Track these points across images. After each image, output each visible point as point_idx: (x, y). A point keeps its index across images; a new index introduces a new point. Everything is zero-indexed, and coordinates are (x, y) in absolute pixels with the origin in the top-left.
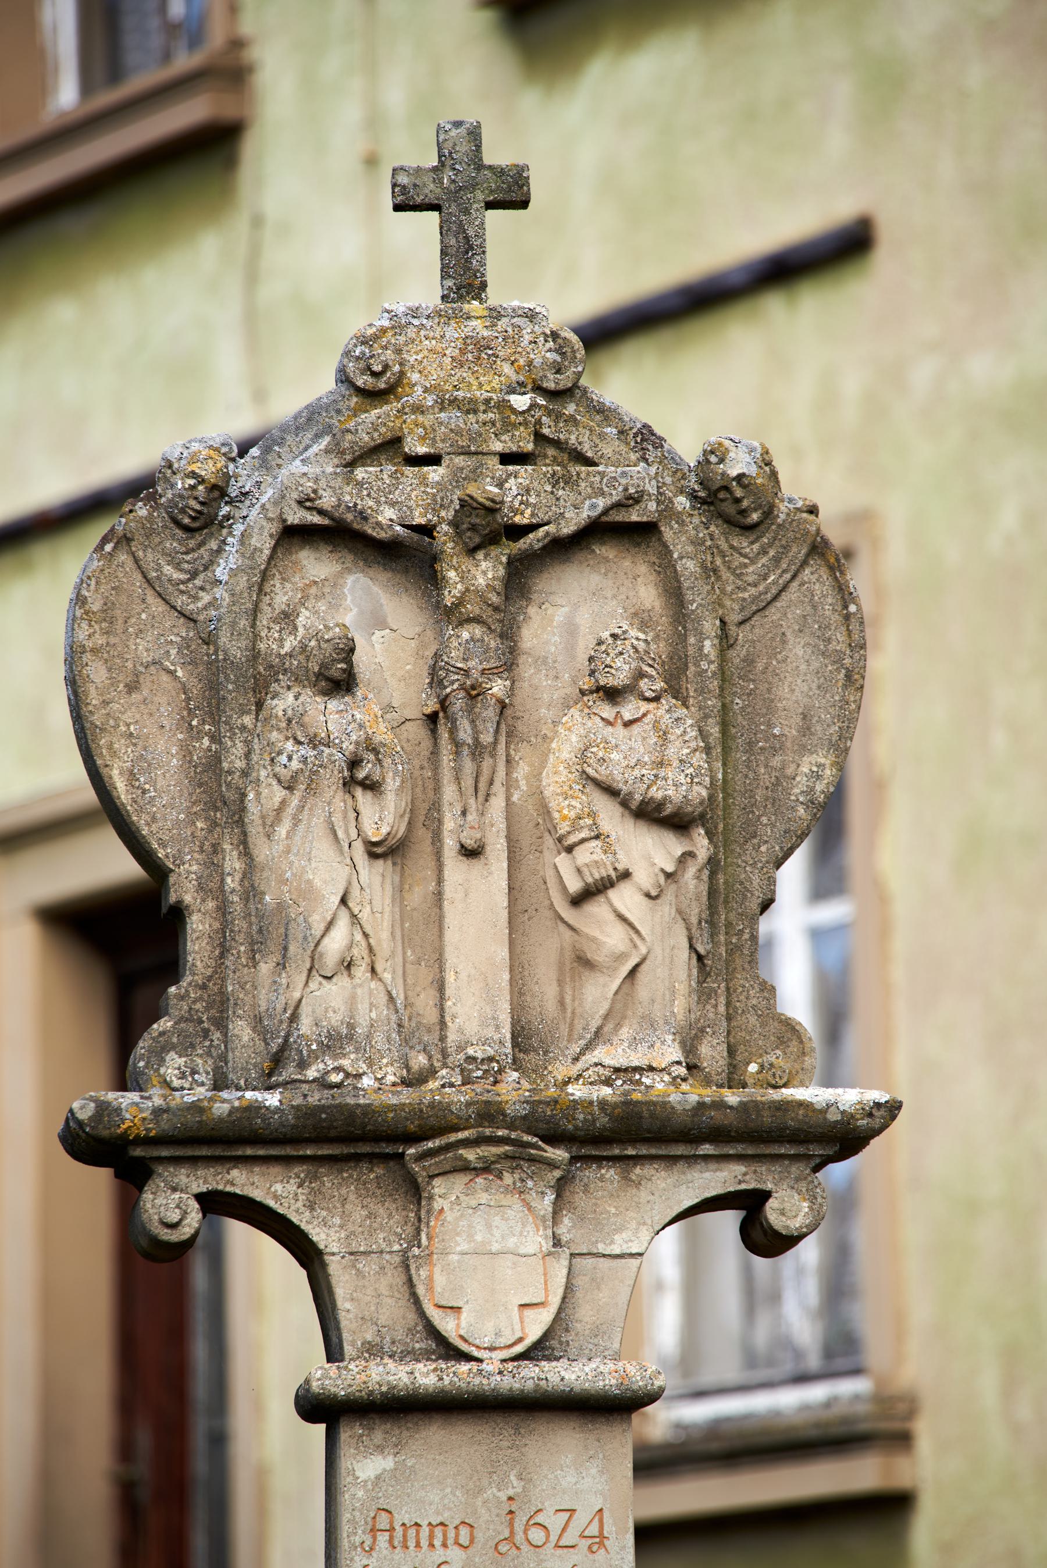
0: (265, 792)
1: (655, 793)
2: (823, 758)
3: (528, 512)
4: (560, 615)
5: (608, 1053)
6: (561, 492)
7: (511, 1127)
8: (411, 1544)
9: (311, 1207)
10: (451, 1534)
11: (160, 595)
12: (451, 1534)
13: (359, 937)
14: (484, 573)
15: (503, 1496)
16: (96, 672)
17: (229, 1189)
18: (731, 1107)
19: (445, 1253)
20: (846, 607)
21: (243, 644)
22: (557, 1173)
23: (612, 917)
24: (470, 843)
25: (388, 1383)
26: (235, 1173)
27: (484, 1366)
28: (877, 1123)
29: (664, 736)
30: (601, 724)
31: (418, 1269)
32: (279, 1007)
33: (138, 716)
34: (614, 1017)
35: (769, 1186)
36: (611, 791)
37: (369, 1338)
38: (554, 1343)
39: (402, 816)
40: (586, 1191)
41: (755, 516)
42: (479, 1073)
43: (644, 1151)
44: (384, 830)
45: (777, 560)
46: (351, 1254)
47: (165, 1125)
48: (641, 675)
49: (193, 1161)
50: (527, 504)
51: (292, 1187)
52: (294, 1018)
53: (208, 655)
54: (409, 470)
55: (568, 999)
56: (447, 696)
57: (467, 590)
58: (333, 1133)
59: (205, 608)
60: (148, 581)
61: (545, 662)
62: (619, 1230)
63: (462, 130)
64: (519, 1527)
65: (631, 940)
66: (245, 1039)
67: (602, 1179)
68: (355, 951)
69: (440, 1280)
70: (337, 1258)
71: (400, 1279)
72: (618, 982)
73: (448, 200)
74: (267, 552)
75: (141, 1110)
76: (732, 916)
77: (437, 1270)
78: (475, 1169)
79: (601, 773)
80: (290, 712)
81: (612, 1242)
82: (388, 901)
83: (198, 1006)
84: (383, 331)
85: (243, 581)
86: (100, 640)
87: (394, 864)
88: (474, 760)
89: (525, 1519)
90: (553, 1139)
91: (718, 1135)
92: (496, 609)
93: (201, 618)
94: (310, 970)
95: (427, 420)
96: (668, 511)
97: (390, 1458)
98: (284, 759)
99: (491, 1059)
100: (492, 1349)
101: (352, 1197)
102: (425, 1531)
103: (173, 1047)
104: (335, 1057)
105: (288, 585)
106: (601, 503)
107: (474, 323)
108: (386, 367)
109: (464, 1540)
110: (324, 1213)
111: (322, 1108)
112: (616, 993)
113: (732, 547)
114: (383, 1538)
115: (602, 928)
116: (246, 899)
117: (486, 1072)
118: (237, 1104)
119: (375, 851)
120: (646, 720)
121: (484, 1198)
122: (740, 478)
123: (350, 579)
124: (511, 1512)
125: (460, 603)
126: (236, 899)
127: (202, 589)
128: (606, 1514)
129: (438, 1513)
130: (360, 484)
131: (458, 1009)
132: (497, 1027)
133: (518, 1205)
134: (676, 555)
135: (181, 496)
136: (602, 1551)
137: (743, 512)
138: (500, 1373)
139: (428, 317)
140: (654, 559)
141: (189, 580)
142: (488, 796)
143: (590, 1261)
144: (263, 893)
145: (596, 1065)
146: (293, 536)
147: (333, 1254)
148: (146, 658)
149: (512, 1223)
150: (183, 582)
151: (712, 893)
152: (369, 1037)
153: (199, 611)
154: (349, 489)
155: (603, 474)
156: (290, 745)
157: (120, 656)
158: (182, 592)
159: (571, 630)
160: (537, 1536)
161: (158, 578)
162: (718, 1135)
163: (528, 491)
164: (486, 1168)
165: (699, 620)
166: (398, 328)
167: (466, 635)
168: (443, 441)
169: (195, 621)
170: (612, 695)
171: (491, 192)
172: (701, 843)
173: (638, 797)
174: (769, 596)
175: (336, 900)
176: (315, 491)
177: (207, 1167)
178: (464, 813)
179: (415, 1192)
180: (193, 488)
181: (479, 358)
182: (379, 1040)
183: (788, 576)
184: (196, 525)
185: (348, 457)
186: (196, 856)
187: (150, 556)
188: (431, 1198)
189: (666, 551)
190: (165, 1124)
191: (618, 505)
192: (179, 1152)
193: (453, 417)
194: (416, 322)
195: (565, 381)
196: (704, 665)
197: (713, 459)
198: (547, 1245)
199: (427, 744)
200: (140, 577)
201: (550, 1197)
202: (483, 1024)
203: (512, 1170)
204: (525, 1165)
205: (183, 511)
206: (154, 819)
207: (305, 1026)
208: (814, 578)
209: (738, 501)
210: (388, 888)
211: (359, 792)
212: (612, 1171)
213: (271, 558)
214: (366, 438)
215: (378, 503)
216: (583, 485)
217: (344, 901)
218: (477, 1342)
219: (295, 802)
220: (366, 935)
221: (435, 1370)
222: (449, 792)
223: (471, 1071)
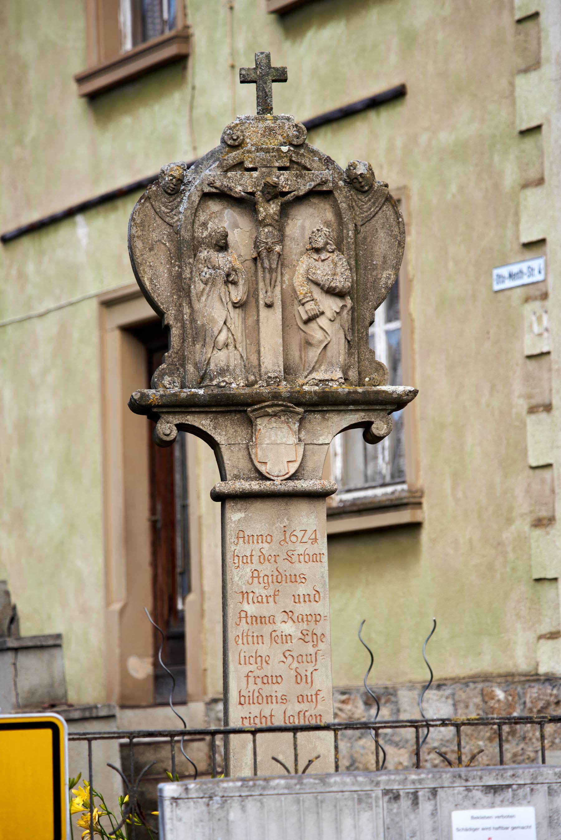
0: (197, 285)
1: (333, 285)
2: (391, 272)
3: (288, 187)
4: (299, 223)
5: (317, 375)
6: (299, 180)
7: (284, 401)
8: (251, 542)
10: (264, 538)
11: (160, 217)
12: (264, 538)
13: (230, 335)
14: (273, 208)
15: (282, 526)
16: (139, 244)
17: (187, 422)
18: (360, 393)
19: (261, 444)
20: (398, 219)
21: (189, 234)
22: (300, 416)
23: (318, 328)
24: (268, 302)
25: (242, 488)
26: (189, 417)
27: (275, 482)
28: (410, 397)
29: (336, 264)
30: (314, 261)
31: (252, 449)
32: (203, 360)
33: (153, 260)
34: (319, 362)
35: (373, 420)
36: (317, 284)
37: (235, 473)
38: (299, 474)
39: (245, 293)
40: (310, 422)
41: (366, 188)
42: (272, 382)
43: (330, 408)
44: (239, 298)
45: (374, 203)
47: (164, 401)
48: (327, 243)
49: (174, 413)
50: (287, 184)
51: (208, 422)
52: (208, 363)
53: (177, 238)
54: (246, 173)
55: (303, 356)
56: (260, 251)
57: (267, 214)
58: (222, 403)
59: (176, 222)
60: (156, 212)
61: (294, 239)
62: (321, 435)
63: (264, 55)
65: (325, 336)
66: (192, 371)
67: (315, 418)
68: (229, 340)
69: (260, 453)
71: (246, 453)
72: (320, 350)
73: (259, 79)
74: (197, 202)
75: (156, 396)
76: (360, 327)
77: (258, 450)
79: (314, 278)
80: (206, 258)
81: (319, 440)
82: (240, 323)
83: (175, 360)
84: (237, 125)
85: (189, 212)
86: (140, 233)
87: (242, 310)
88: (269, 274)
89: (289, 533)
90: (298, 404)
91: (355, 402)
92: (277, 221)
93: (175, 225)
94: (214, 347)
95: (252, 155)
96: (336, 186)
97: (243, 513)
98: (204, 274)
99: (276, 377)
100: (278, 476)
101: (229, 425)
102: (255, 538)
103: (167, 374)
104: (223, 377)
105: (205, 213)
106: (313, 184)
107: (268, 122)
108: (238, 137)
109: (269, 540)
110: (219, 431)
111: (218, 395)
112: (320, 354)
113: (359, 199)
114: (241, 540)
115: (315, 332)
116: (191, 322)
117: (275, 382)
118: (189, 393)
119: (236, 306)
120: (329, 259)
121: (274, 425)
122: (361, 174)
123: (226, 211)
124: (285, 531)
125: (264, 219)
126: (188, 323)
127: (175, 215)
128: (317, 531)
129: (260, 532)
130: (229, 178)
131: (265, 360)
132: (279, 366)
133: (286, 427)
134: (339, 202)
135: (167, 183)
136: (316, 544)
137: (362, 187)
138: (281, 484)
139: (252, 120)
140: (331, 203)
141: (170, 212)
142: (274, 287)
143: (311, 446)
144: (197, 321)
145: (313, 379)
146: (206, 196)
148: (156, 239)
149: (284, 433)
150: (168, 213)
151: (353, 319)
152: (234, 370)
153: (174, 223)
154: (225, 180)
155: (313, 174)
156: (206, 269)
157: (147, 239)
158: (168, 216)
159: (303, 228)
160: (294, 539)
161: (160, 211)
162: (355, 402)
163: (288, 180)
164: (275, 415)
165: (347, 224)
166: (242, 124)
167: (266, 230)
168: (258, 163)
169: (173, 226)
170: (317, 251)
171: (274, 76)
172: (349, 302)
173: (327, 286)
174: (371, 216)
175: (222, 323)
176: (214, 181)
177: (179, 415)
178: (266, 292)
179: (251, 423)
180: (171, 180)
181: (270, 134)
182: (238, 371)
183: (378, 209)
184: (173, 193)
185: (225, 169)
186: (174, 308)
187: (157, 204)
188: (256, 425)
189: (336, 200)
190: (164, 400)
191: (319, 185)
192: (169, 410)
193: (262, 154)
194: (248, 121)
195: (300, 141)
196: (349, 240)
197: (352, 168)
198: (296, 441)
199: (253, 268)
200: (153, 211)
202: (274, 365)
203: (284, 415)
205: (168, 188)
206: (159, 295)
207: (212, 366)
208: (387, 209)
209: (360, 183)
210: (240, 318)
211: (230, 285)
212: (319, 415)
213: (199, 204)
214: (231, 162)
215: (236, 184)
216: (307, 177)
217: (225, 323)
218: (273, 474)
219: (208, 289)
220: (233, 335)
221: (258, 484)
222: (261, 285)
223: (270, 381)
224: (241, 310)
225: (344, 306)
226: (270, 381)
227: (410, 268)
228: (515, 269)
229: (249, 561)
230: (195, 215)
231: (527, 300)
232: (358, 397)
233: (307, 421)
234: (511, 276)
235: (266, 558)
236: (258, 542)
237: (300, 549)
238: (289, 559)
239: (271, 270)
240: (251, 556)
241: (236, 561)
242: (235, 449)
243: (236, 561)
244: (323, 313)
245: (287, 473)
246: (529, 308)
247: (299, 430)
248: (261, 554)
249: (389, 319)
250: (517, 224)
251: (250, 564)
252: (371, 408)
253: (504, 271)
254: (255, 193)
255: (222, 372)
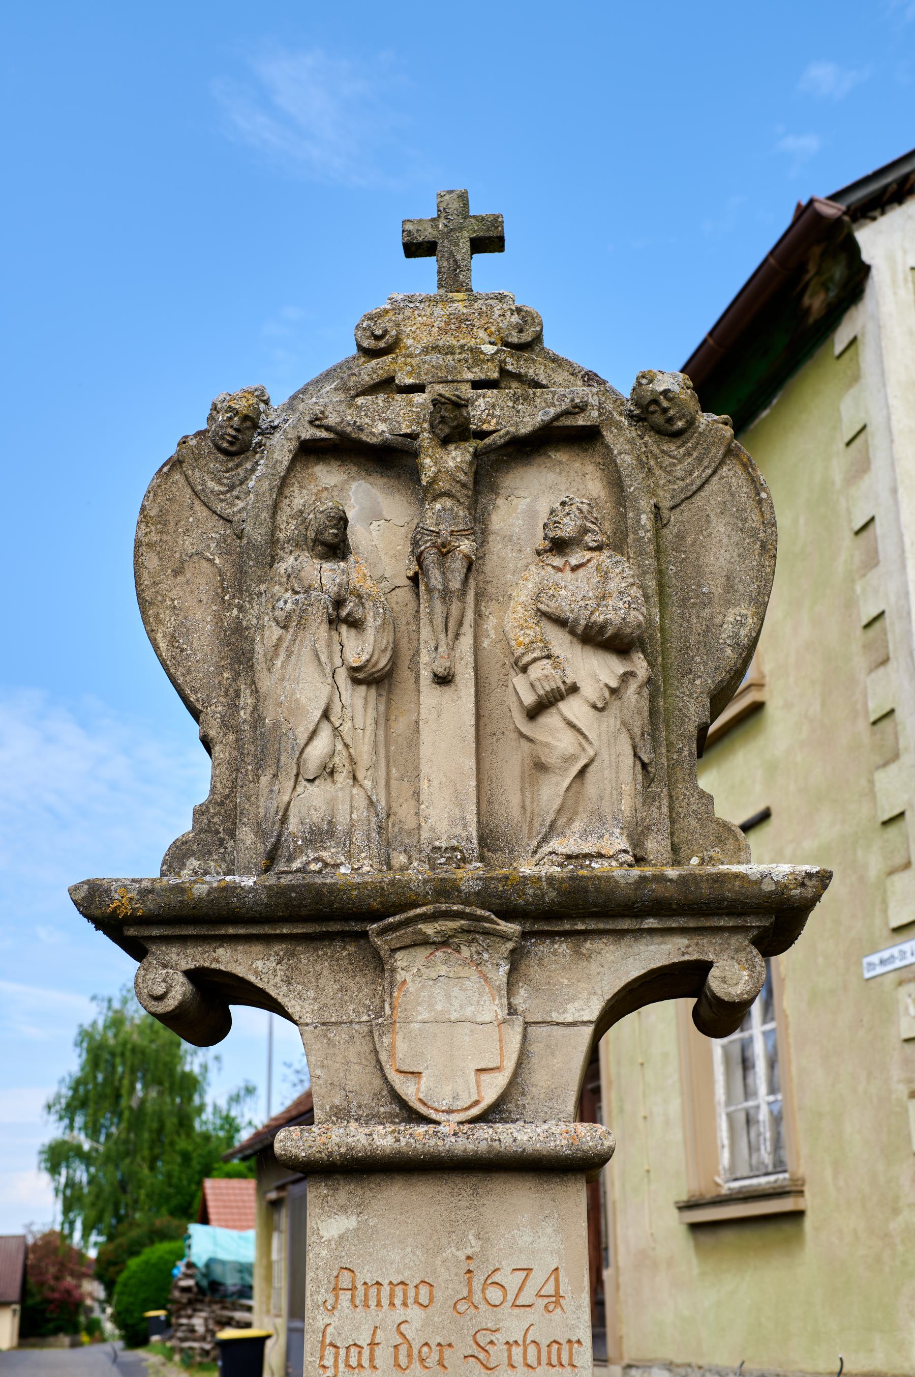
0: (267, 633)
1: (598, 618)
2: (746, 610)
3: (494, 421)
4: (522, 505)
5: (561, 843)
6: (520, 407)
7: (467, 903)
8: (373, 1303)
9: (288, 981)
10: (411, 1293)
11: (204, 503)
12: (411, 1293)
13: (340, 747)
14: (454, 458)
15: (462, 1255)
16: (152, 561)
17: (214, 966)
18: (671, 880)
19: (407, 1022)
20: (759, 494)
21: (263, 531)
22: (510, 945)
23: (562, 724)
24: (440, 671)
25: (347, 1144)
26: (220, 951)
27: (441, 1128)
28: (809, 892)
29: (605, 576)
30: (552, 571)
31: (381, 1036)
32: (273, 811)
33: (181, 594)
34: (566, 810)
35: (711, 957)
36: (560, 622)
37: (337, 1102)
38: (511, 1107)
39: (384, 651)
40: (541, 964)
41: (680, 424)
42: (443, 860)
43: (592, 925)
44: (365, 657)
45: (700, 460)
46: (323, 1024)
47: (151, 906)
48: (586, 531)
49: (183, 940)
50: (493, 416)
51: (272, 964)
52: (284, 820)
53: (240, 546)
54: (398, 397)
55: (528, 803)
56: (422, 553)
57: (439, 471)
58: (304, 912)
59: (240, 511)
60: (195, 493)
61: (510, 540)
62: (572, 999)
63: (454, 196)
64: (477, 1285)
65: (580, 744)
66: (249, 842)
67: (555, 954)
68: (337, 759)
69: (402, 1047)
70: (311, 1028)
71: (367, 1048)
72: (568, 780)
73: (442, 238)
74: (286, 463)
75: (128, 891)
76: (673, 737)
77: (399, 1038)
78: (434, 943)
79: (550, 606)
80: (290, 570)
81: (565, 1011)
82: (370, 721)
83: (216, 820)
84: (386, 311)
85: (266, 485)
86: (154, 537)
87: (379, 695)
88: (444, 601)
89: (483, 1278)
90: (507, 914)
91: (660, 908)
92: (464, 485)
93: (236, 519)
94: (297, 775)
95: (414, 362)
96: (611, 422)
97: (354, 1218)
98: (281, 604)
99: (454, 849)
100: (449, 1112)
101: (326, 972)
102: (386, 1290)
103: (193, 854)
104: (316, 850)
105: (305, 491)
106: (552, 411)
107: (456, 305)
108: (386, 332)
109: (424, 1299)
110: (300, 987)
111: (292, 888)
112: (567, 790)
113: (663, 452)
114: (345, 1297)
115: (552, 732)
116: (254, 728)
117: (448, 859)
118: (215, 885)
119: (360, 676)
120: (590, 565)
121: (443, 970)
122: (666, 392)
123: (354, 485)
124: (469, 1271)
125: (433, 481)
126: (247, 727)
127: (238, 498)
128: (562, 1273)
129: (398, 1272)
130: (359, 408)
131: (431, 812)
132: (465, 827)
133: (475, 977)
134: (615, 452)
135: (221, 427)
136: (558, 1310)
137: (670, 420)
138: (455, 1134)
139: (421, 302)
140: (598, 460)
141: (228, 491)
142: (457, 636)
143: (544, 1030)
144: (265, 719)
145: (551, 853)
146: (310, 451)
148: (191, 550)
149: (470, 993)
150: (222, 493)
151: (653, 713)
152: (349, 834)
153: (234, 514)
154: (350, 411)
155: (554, 393)
156: (288, 595)
157: (171, 549)
158: (222, 500)
159: (532, 513)
160: (494, 1294)
161: (203, 490)
162: (660, 908)
163: (494, 407)
164: (444, 942)
165: (636, 499)
166: (397, 310)
167: (438, 506)
168: (426, 374)
169: (231, 522)
170: (559, 546)
171: (475, 231)
172: (640, 665)
173: (583, 622)
174: (694, 487)
175: (318, 714)
176: (322, 412)
177: (196, 946)
178: (436, 649)
179: (379, 965)
180: (230, 419)
181: (460, 327)
182: (358, 838)
183: (709, 471)
184: (233, 449)
185: (352, 393)
186: (221, 699)
187: (197, 474)
188: (393, 970)
189: (609, 450)
190: (151, 904)
191: (566, 413)
192: (168, 931)
193: (435, 358)
194: (412, 305)
195: (526, 337)
196: (641, 533)
197: (644, 381)
198: (502, 1013)
199: (412, 605)
200: (190, 491)
201: (505, 968)
202: (453, 824)
203: (470, 943)
204: (480, 938)
205: (222, 438)
206: (189, 671)
207: (293, 825)
208: (731, 474)
209: (665, 410)
210: (371, 713)
211: (344, 629)
212: (564, 946)
213: (290, 469)
214: (367, 378)
215: (373, 420)
216: (538, 400)
217: (326, 715)
218: (436, 1105)
219: (289, 637)
220: (346, 746)
221: (393, 1132)
222: (425, 632)
223: (435, 859)
224: (373, 691)
225: (627, 676)
226: (435, 859)
227: (782, 968)
228: (885, 954)
229: (365, 1362)
230: (280, 492)
231: (900, 983)
232: (670, 892)
233: (533, 961)
234: (882, 962)
235: (415, 1352)
236: (392, 1304)
237: (513, 1326)
238: (482, 1355)
239: (446, 595)
240: (373, 1344)
241: (329, 1362)
242: (340, 1035)
243: (329, 1362)
244: (574, 689)
245: (476, 1103)
246: (903, 991)
247: (511, 986)
248: (400, 1341)
249: (765, 1021)
250: (885, 911)
251: (368, 1372)
252: (708, 937)
253: (875, 958)
254: (418, 435)
255: (319, 835)
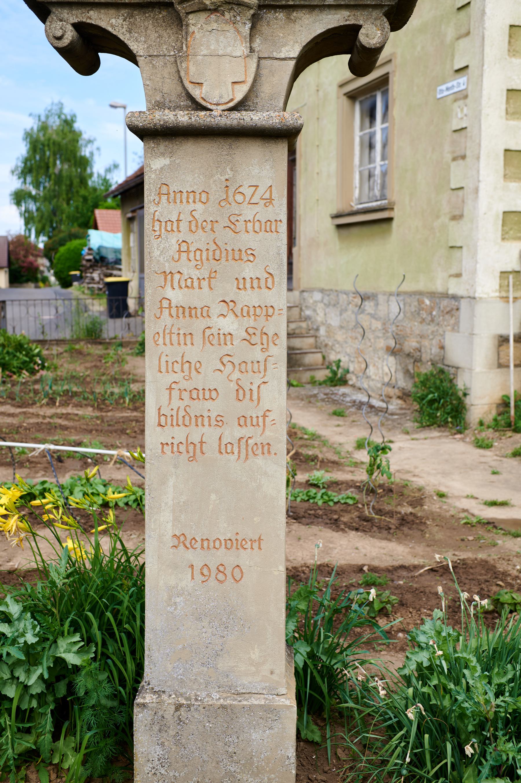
8: (178, 201)
9: (130, 31)
10: (198, 196)
12: (198, 196)
15: (223, 178)
17: (89, 21)
22: (252, 12)
26: (91, 13)
31: (181, 63)
35: (361, 23)
38: (250, 103)
40: (268, 24)
46: (150, 56)
51: (120, 21)
64: (231, 193)
67: (276, 19)
69: (192, 69)
70: (143, 58)
71: (174, 70)
77: (191, 64)
78: (210, 10)
81: (280, 52)
97: (168, 159)
100: (217, 104)
101: (150, 27)
102: (185, 195)
109: (204, 199)
110: (136, 35)
114: (164, 198)
121: (215, 26)
124: (227, 186)
128: (273, 188)
129: (191, 186)
133: (232, 30)
136: (271, 206)
138: (220, 116)
147: (141, 56)
177: (78, 9)
179: (179, 23)
188: (187, 25)
198: (247, 51)
201: (249, 25)
204: (236, 7)
212: (281, 14)
218: (210, 101)
227: (395, 93)
228: (449, 85)
229: (175, 229)
231: (455, 100)
233: (264, 23)
234: (448, 89)
235: (200, 224)
236: (188, 202)
237: (248, 213)
238: (232, 227)
240: (178, 221)
241: (157, 228)
242: (159, 63)
243: (157, 228)
245: (232, 100)
246: (456, 104)
247: (252, 36)
248: (192, 219)
249: (383, 122)
250: (452, 60)
251: (176, 233)
253: (444, 87)
